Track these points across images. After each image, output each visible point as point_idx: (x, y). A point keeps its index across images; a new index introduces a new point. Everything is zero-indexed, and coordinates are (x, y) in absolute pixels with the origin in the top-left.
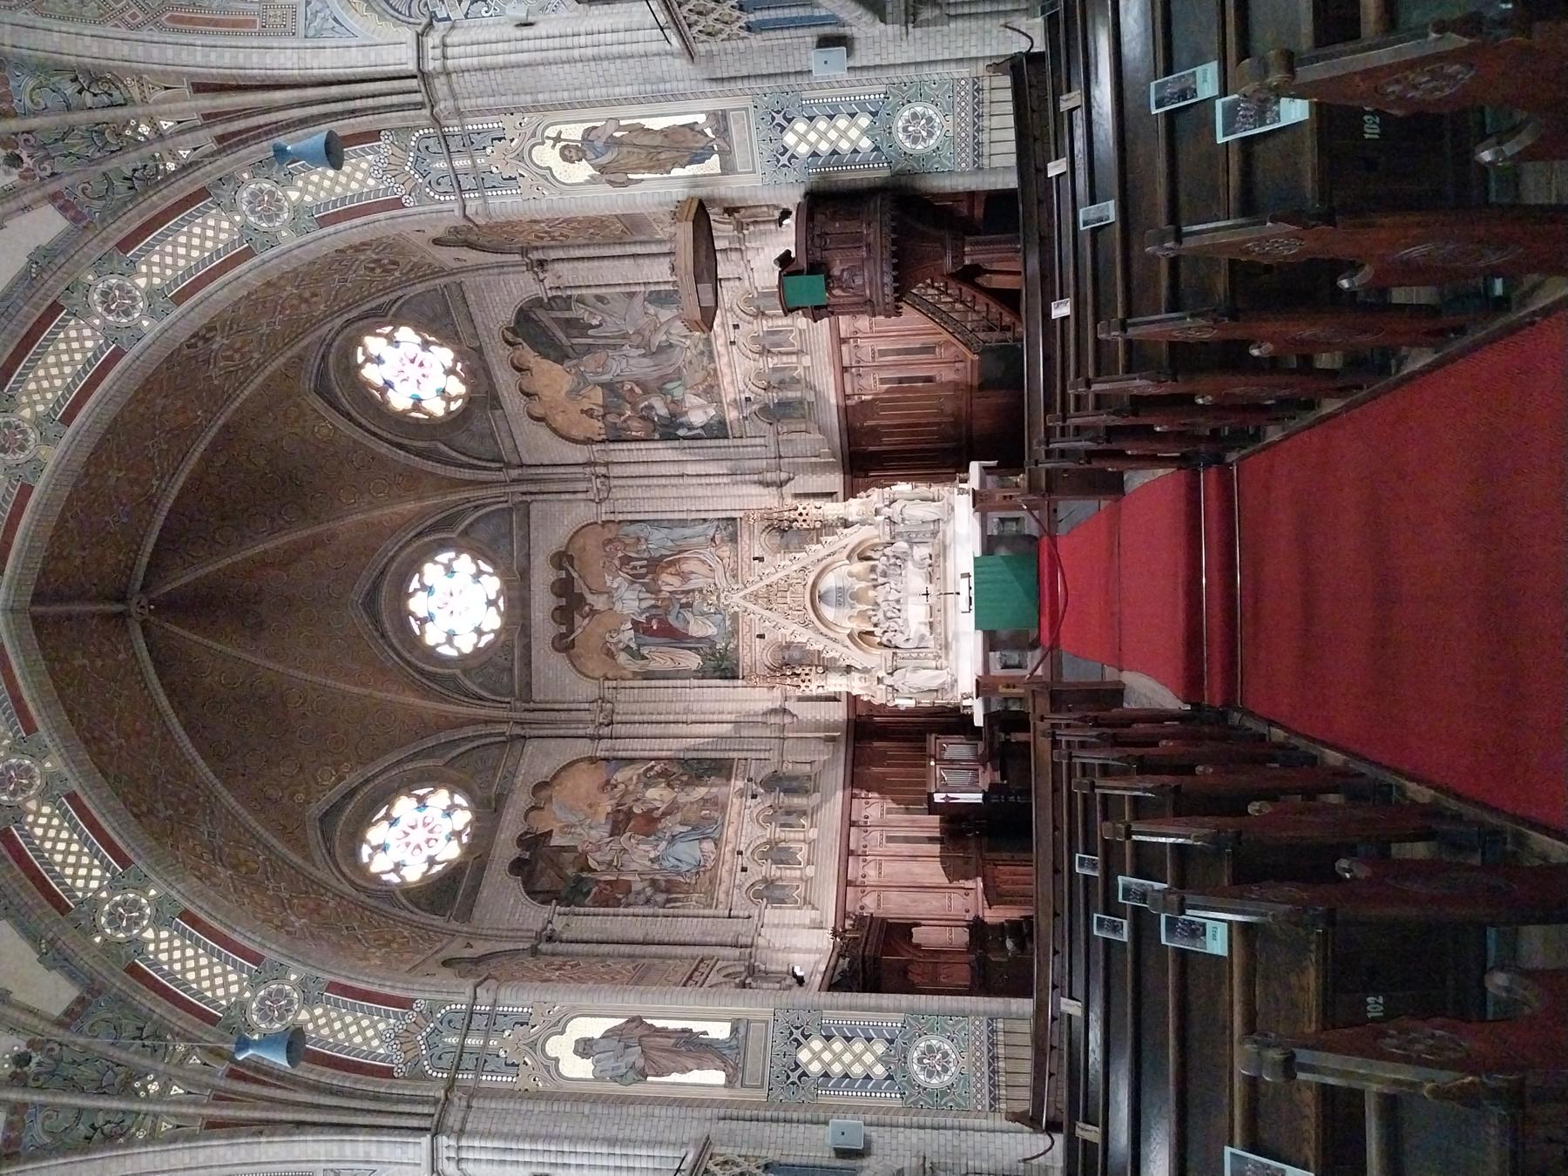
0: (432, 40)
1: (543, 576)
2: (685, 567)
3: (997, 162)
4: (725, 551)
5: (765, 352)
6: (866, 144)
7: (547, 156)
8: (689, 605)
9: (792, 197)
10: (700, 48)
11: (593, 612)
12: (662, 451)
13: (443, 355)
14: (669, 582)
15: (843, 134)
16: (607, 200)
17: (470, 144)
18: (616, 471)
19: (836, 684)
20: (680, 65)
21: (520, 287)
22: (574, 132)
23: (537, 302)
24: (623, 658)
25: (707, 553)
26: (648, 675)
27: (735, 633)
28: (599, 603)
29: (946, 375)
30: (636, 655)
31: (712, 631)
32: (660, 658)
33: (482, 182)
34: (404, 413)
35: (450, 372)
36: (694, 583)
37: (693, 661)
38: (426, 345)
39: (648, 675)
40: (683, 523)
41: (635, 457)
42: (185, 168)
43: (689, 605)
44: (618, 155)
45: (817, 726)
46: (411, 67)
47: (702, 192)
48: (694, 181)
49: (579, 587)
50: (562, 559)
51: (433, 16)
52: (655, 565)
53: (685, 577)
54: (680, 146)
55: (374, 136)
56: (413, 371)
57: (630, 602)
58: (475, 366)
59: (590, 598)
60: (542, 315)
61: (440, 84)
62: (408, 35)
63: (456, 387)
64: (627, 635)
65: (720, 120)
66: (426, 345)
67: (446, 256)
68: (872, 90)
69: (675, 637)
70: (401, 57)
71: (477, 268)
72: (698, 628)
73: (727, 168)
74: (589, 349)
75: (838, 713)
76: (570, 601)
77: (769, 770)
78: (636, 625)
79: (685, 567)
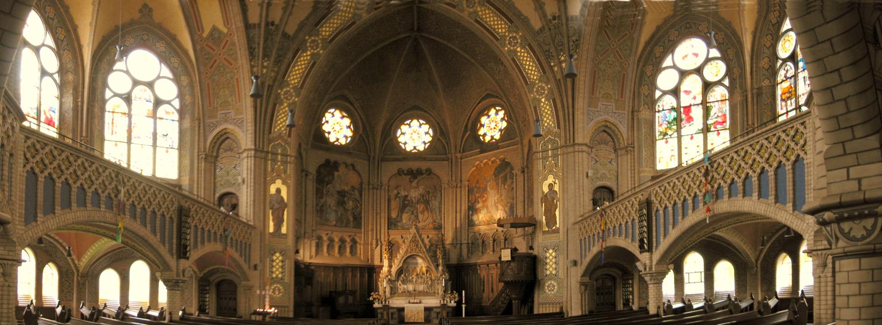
0: (585, 148)
1: (424, 165)
2: (426, 213)
3: (541, 309)
4: (431, 226)
5: (494, 241)
6: (548, 273)
7: (550, 179)
8: (413, 213)
9: (535, 252)
10: (577, 226)
11: (411, 182)
12: (465, 206)
13: (497, 136)
14: (421, 207)
15: (551, 266)
16: (537, 197)
17: (555, 156)
18: (458, 190)
19: (386, 263)
20: (572, 220)
21: (517, 163)
22: (556, 188)
23: (512, 169)
24: (395, 192)
25: (430, 220)
26: (389, 200)
27: (403, 229)
28: (414, 184)
29: (485, 295)
30: (397, 196)
31: (404, 221)
32: (395, 204)
33: (545, 158)
34: (480, 121)
35: (492, 137)
36: (420, 217)
37: (394, 215)
38: (501, 130)
39: (389, 200)
40: (440, 211)
41: (463, 200)
42: (551, 68)
43: (413, 213)
44: (550, 200)
45: (372, 256)
46: (576, 142)
47: (538, 225)
48: (541, 222)
49: (420, 177)
50: (429, 172)
51: (592, 148)
52: (427, 203)
53: (422, 212)
54: (551, 220)
55: (559, 127)
56: (493, 125)
57: (414, 194)
58: (493, 145)
59: (416, 181)
60: (508, 170)
61: (570, 149)
62: (587, 141)
63: (488, 139)
64: (403, 193)
65: (557, 231)
66: (501, 130)
67: (526, 142)
68: (561, 275)
69: (402, 210)
70: (579, 139)
71: (523, 150)
72: (405, 217)
73: (544, 233)
74: (498, 184)
75: (377, 262)
76: (414, 174)
77: (358, 241)
78: (406, 196)
79: (426, 213)
